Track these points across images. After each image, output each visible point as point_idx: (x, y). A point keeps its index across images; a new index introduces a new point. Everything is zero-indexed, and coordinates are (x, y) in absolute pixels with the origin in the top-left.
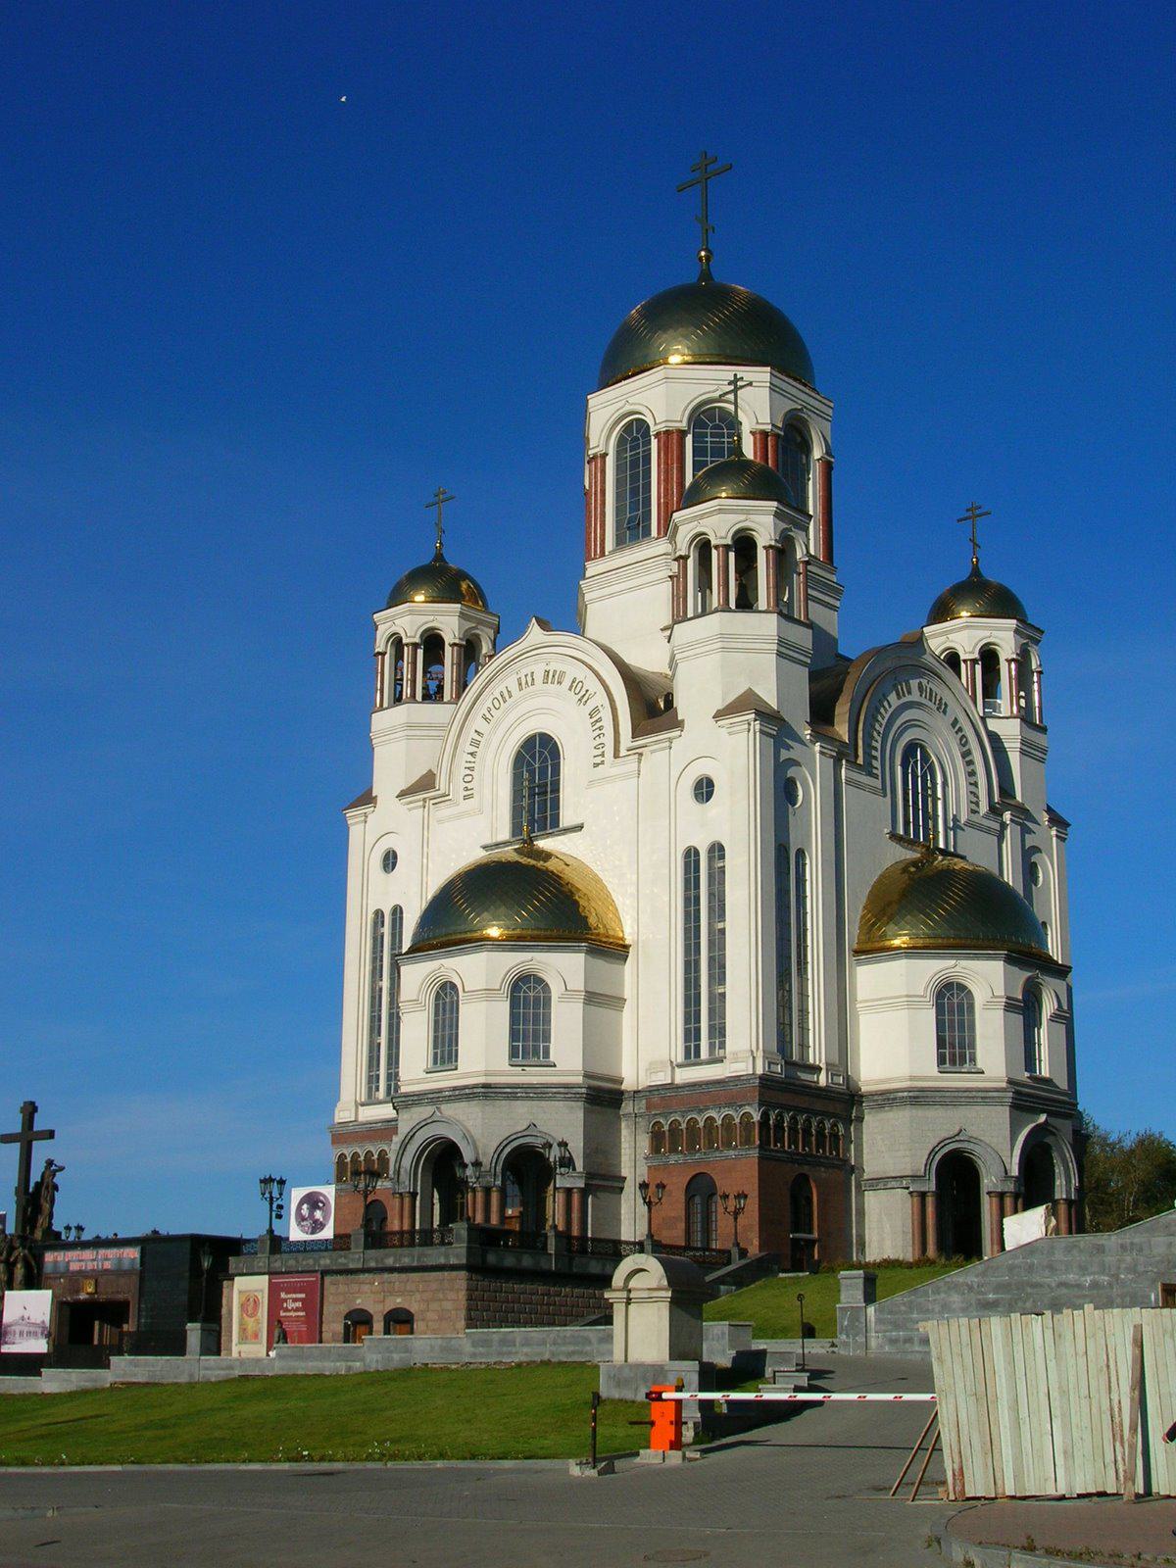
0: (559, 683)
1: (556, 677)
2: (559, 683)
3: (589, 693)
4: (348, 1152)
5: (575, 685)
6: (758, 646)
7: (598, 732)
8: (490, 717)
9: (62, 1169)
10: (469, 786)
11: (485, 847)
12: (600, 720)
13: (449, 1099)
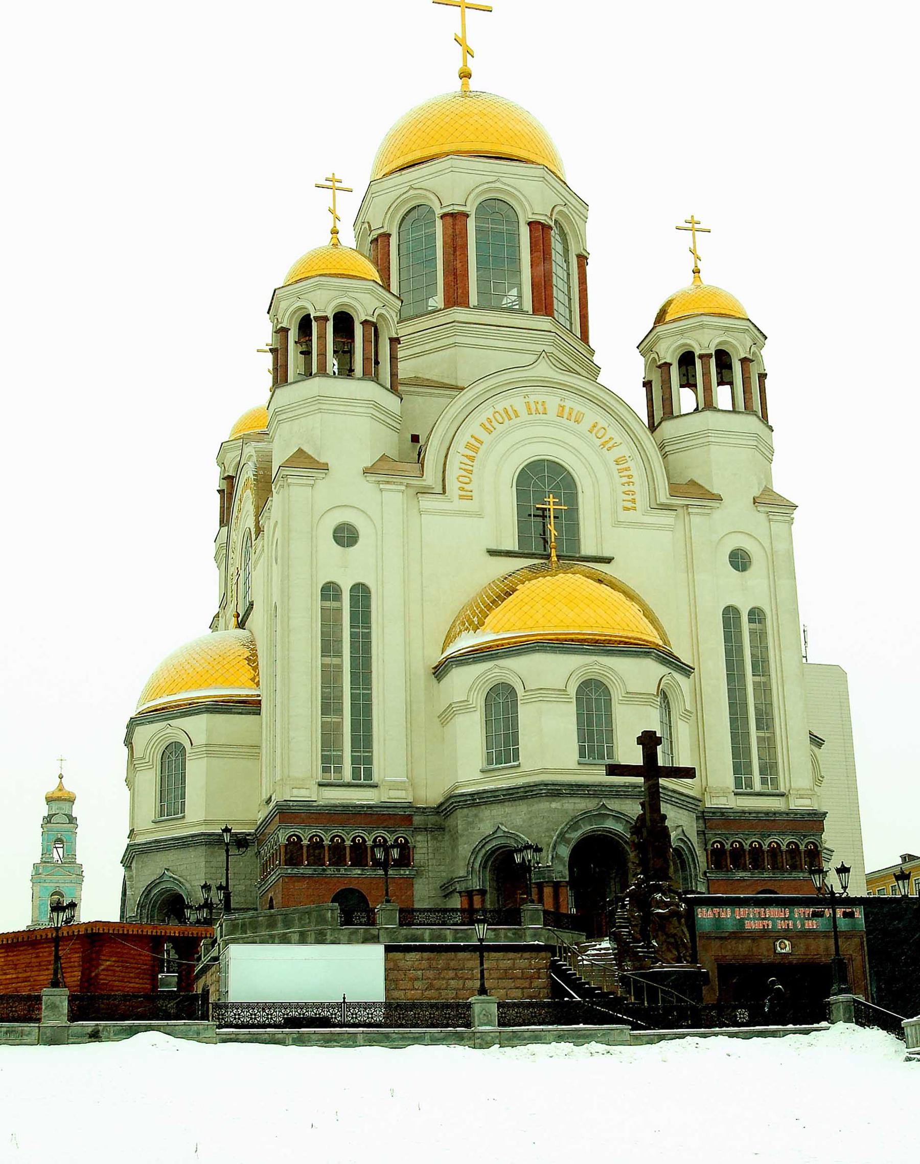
5: (596, 429)
7: (625, 480)
10: (467, 487)
11: (493, 553)
12: (628, 469)
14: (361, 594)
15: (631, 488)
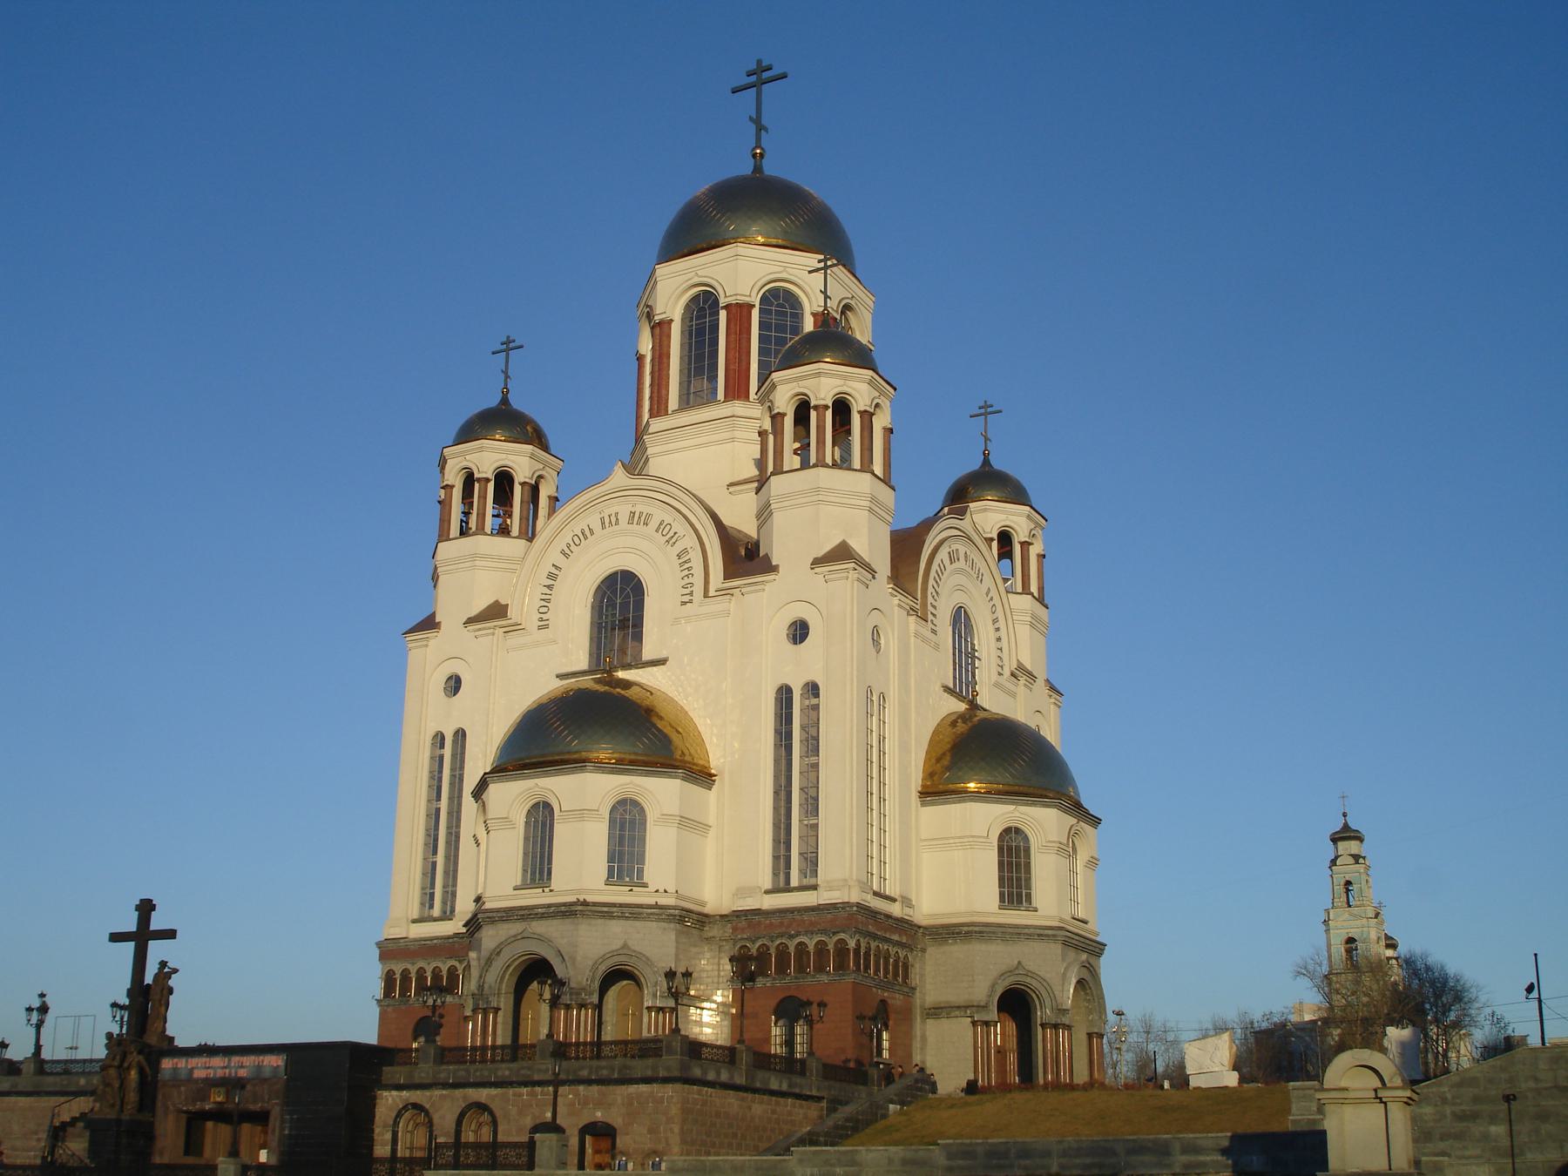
0: (646, 524)
1: (643, 519)
2: (646, 524)
3: (677, 536)
4: (398, 968)
5: (662, 527)
6: (853, 502)
7: (686, 572)
8: (569, 552)
9: (175, 971)
11: (561, 676)
13: (542, 917)
14: (460, 735)
15: (690, 580)
